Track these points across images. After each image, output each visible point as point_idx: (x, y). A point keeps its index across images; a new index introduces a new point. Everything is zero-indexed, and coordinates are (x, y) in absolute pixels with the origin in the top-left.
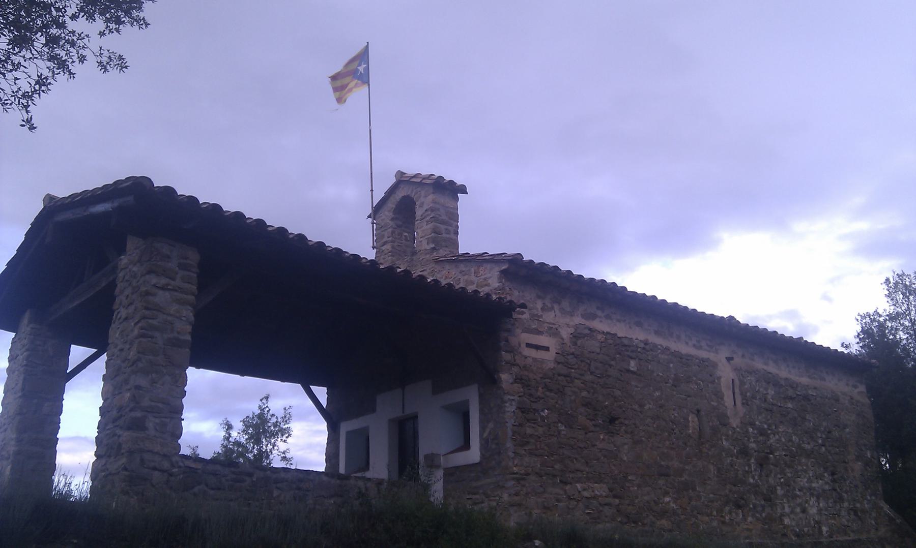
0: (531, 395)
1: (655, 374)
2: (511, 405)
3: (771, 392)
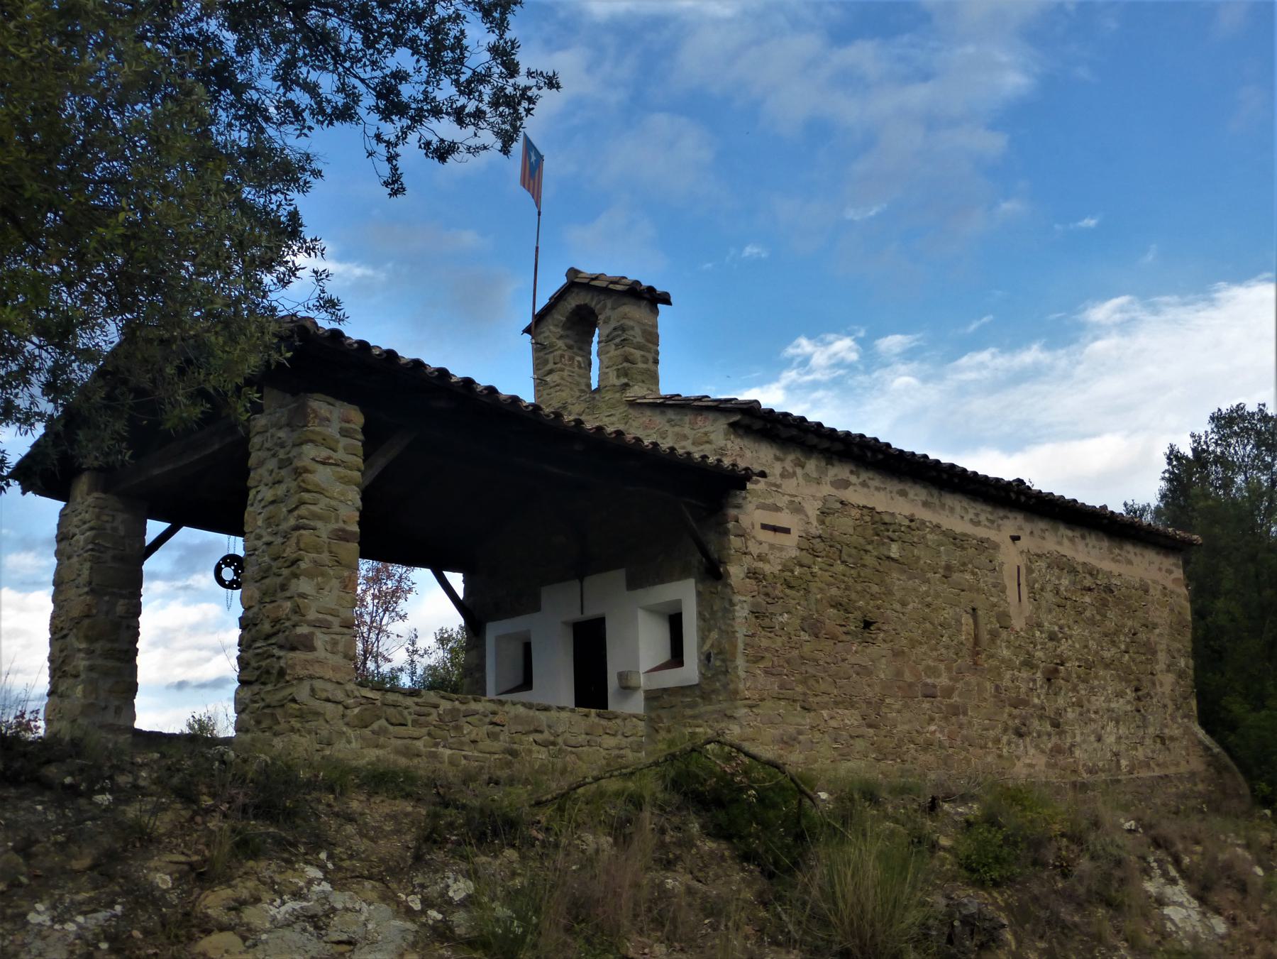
0: (767, 595)
1: (922, 562)
2: (743, 608)
3: (1065, 582)
